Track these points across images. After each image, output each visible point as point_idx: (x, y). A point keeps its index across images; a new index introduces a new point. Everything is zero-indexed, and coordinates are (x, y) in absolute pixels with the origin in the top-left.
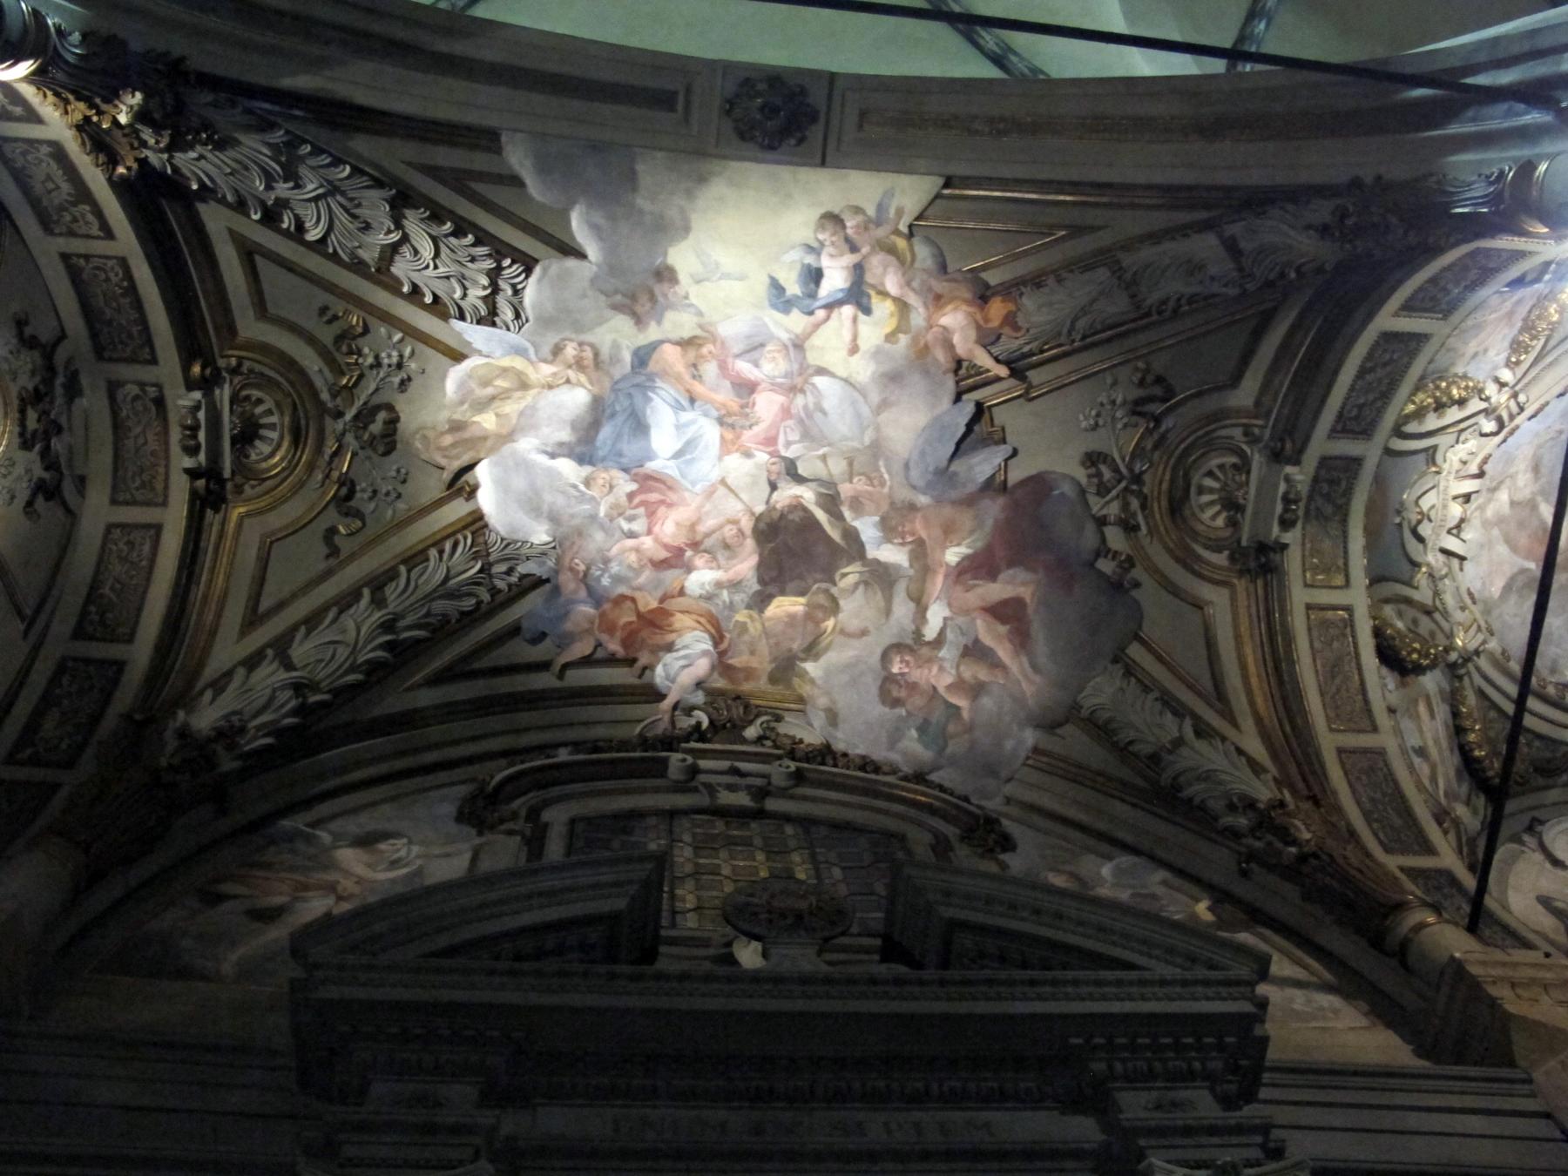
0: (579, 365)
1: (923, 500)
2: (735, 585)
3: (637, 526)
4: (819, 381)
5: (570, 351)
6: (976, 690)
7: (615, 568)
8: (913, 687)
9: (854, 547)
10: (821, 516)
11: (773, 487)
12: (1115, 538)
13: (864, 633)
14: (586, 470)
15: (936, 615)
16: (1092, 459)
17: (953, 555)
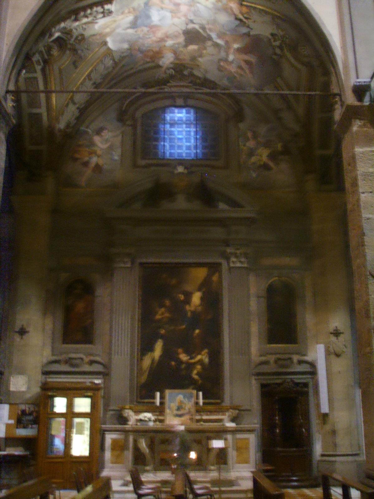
0: (129, 12)
1: (228, 33)
2: (178, 44)
3: (150, 36)
4: (198, 5)
5: (126, 11)
7: (146, 45)
8: (226, 69)
9: (210, 38)
10: (201, 31)
11: (187, 24)
12: (278, 51)
13: (213, 55)
14: (135, 30)
16: (272, 35)
17: (236, 46)
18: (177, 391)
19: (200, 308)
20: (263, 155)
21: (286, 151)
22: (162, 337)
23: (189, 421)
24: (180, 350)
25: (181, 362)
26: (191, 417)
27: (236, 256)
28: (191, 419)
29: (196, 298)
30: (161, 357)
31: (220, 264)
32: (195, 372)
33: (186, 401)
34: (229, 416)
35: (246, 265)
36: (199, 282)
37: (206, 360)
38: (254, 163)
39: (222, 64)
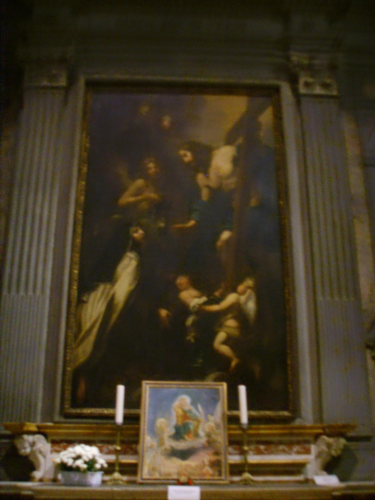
18: (172, 386)
19: (232, 183)
22: (136, 247)
23: (208, 470)
24: (182, 280)
25: (183, 310)
26: (214, 458)
27: (311, 69)
28: (216, 465)
29: (223, 160)
30: (131, 295)
31: (277, 90)
32: (221, 336)
33: (199, 411)
34: (318, 456)
35: (335, 93)
36: (228, 125)
37: (251, 306)
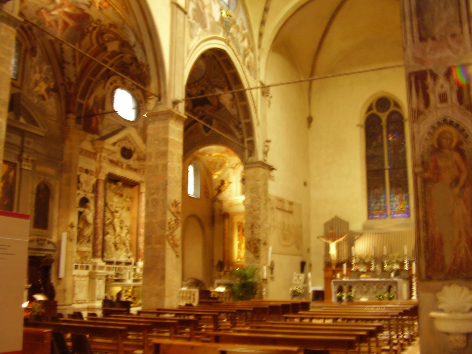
6: (51, 26)
15: (55, 13)
17: (67, 10)
20: (42, 88)
21: (55, 89)
38: (37, 92)
39: (43, 11)
